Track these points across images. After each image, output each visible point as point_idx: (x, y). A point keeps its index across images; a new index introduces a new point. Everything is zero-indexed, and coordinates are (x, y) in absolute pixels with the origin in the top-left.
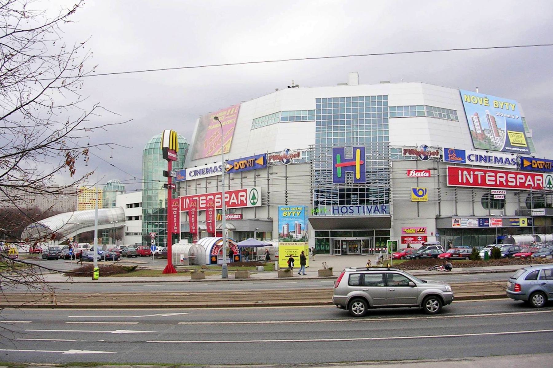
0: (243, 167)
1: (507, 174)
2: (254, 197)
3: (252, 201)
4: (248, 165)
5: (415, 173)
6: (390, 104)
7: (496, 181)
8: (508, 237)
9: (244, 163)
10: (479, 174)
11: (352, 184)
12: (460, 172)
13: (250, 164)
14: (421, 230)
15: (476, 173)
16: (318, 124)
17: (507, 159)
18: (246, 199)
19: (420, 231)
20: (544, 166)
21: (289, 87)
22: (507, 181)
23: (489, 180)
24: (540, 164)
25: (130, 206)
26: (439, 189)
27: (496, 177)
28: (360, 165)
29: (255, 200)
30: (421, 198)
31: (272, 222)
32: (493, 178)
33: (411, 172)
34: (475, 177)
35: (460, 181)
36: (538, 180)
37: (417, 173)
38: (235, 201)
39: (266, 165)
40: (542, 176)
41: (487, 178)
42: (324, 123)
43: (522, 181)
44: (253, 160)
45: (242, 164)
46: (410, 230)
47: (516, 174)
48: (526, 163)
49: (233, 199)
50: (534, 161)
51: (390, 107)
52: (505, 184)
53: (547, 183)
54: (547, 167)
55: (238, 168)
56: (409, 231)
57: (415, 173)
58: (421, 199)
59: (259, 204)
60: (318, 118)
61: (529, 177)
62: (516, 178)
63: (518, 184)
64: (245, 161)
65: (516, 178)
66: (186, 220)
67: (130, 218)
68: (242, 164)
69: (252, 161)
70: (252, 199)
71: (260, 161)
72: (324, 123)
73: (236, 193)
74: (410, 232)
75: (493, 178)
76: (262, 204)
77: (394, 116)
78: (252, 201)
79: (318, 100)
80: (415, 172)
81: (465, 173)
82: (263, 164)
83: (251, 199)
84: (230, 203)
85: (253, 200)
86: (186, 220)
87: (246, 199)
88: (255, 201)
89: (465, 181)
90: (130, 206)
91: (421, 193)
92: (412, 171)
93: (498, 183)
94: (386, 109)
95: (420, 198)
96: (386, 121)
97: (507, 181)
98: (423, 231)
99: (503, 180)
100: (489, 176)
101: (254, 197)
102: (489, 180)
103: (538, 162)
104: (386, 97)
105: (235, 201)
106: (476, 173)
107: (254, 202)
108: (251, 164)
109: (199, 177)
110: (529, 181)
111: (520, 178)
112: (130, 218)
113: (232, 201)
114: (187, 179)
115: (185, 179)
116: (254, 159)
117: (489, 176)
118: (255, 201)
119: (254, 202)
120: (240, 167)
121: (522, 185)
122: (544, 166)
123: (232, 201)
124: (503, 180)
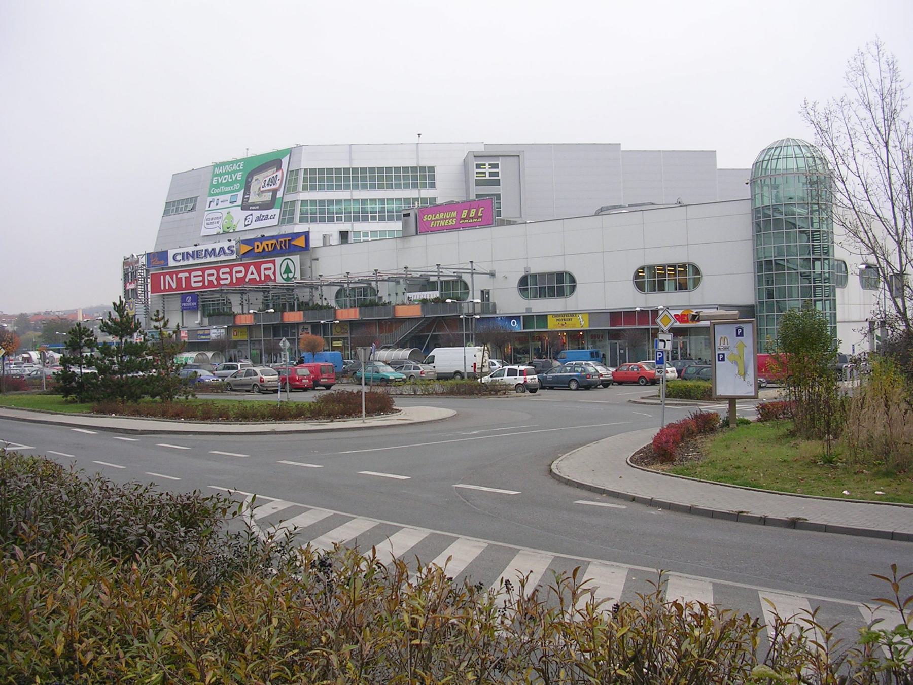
0: (270, 250)
3: (285, 276)
9: (272, 244)
18: (274, 273)
29: (289, 274)
38: (256, 276)
44: (287, 239)
45: (267, 245)
49: (252, 273)
64: (274, 241)
68: (267, 245)
69: (285, 241)
78: (285, 276)
83: (282, 273)
84: (247, 280)
85: (286, 275)
87: (274, 273)
88: (291, 275)
105: (256, 276)
107: (288, 276)
113: (249, 276)
116: (290, 238)
118: (291, 275)
119: (288, 276)
123: (249, 276)
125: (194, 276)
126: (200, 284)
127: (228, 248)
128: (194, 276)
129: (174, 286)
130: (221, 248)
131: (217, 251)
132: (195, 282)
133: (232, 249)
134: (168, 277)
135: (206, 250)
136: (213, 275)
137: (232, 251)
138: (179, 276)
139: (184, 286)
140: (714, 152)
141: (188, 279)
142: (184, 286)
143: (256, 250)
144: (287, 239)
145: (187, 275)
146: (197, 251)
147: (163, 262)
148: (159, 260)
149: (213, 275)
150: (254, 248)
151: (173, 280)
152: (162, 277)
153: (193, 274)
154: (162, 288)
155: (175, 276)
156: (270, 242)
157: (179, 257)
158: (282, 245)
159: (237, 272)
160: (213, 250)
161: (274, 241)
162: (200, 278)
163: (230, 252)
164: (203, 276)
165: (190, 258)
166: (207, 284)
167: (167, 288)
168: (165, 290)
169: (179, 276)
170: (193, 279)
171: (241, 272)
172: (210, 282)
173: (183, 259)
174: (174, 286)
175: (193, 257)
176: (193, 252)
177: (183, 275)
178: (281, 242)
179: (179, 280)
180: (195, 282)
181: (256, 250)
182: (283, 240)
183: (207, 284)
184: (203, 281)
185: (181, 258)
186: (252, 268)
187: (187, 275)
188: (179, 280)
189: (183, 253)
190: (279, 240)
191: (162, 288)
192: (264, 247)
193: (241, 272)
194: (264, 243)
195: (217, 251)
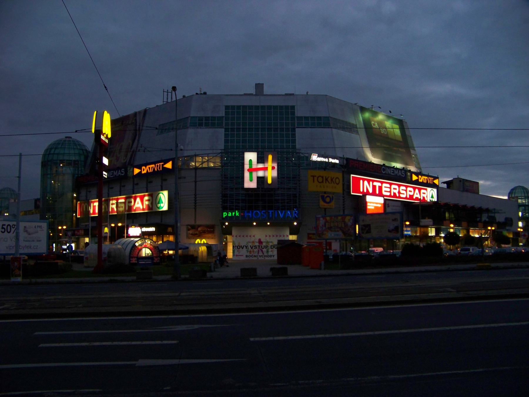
0: (151, 171)
7: (390, 192)
9: (152, 167)
12: (361, 181)
15: (375, 183)
16: (226, 130)
22: (399, 193)
23: (385, 191)
24: (424, 179)
26: (343, 197)
27: (390, 188)
30: (329, 204)
32: (389, 190)
34: (374, 187)
35: (361, 190)
36: (424, 193)
40: (426, 189)
41: (384, 189)
42: (233, 130)
43: (412, 194)
51: (297, 117)
52: (397, 195)
53: (430, 197)
54: (430, 182)
60: (227, 124)
61: (417, 191)
62: (406, 191)
63: (408, 197)
65: (406, 191)
69: (160, 165)
72: (233, 130)
75: (389, 190)
77: (300, 126)
79: (227, 107)
81: (366, 182)
91: (328, 200)
93: (392, 194)
94: (293, 119)
95: (327, 205)
96: (294, 130)
97: (399, 193)
99: (396, 192)
100: (385, 187)
102: (385, 191)
104: (293, 107)
106: (375, 183)
110: (417, 194)
111: (410, 191)
117: (385, 187)
124: (396, 192)
144: (161, 164)
161: (153, 166)
182: (158, 164)
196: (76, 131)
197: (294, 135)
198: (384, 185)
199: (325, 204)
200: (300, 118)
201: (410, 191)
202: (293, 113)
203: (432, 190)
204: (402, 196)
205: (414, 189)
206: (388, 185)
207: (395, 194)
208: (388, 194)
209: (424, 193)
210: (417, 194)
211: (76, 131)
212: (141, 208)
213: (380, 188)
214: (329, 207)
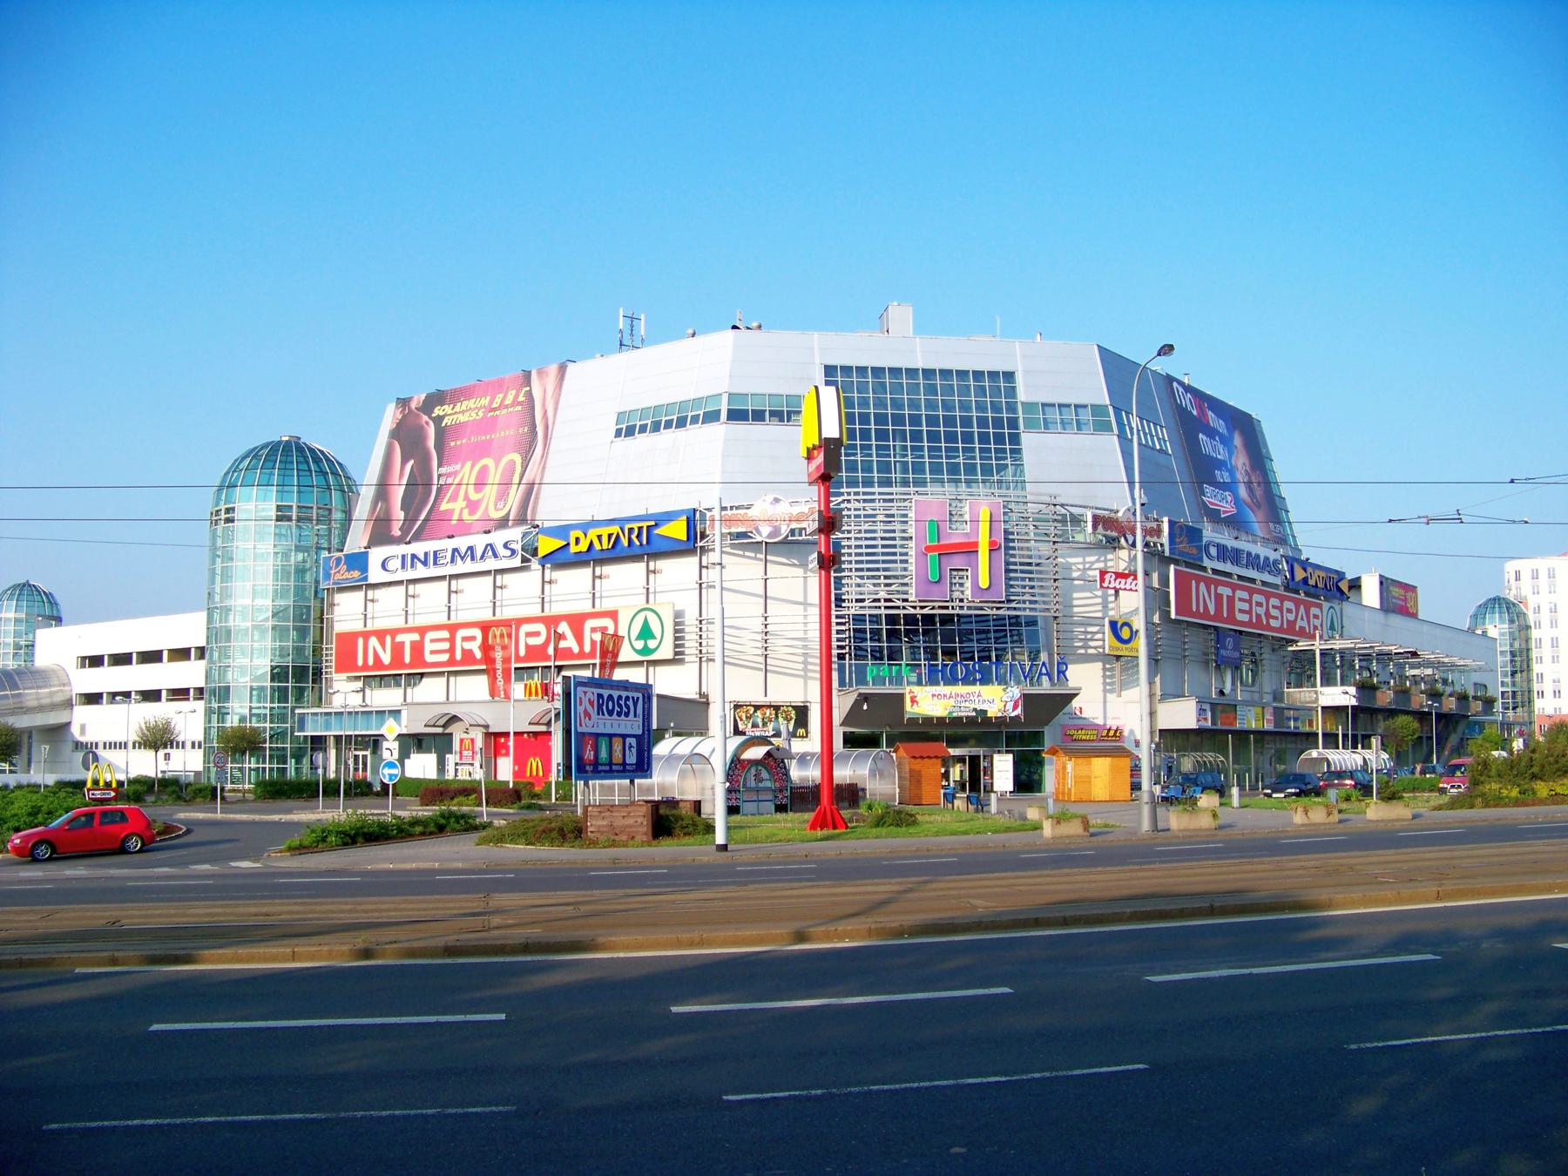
0: (605, 547)
1: (1268, 596)
2: (646, 632)
3: (639, 645)
4: (625, 542)
5: (1115, 580)
6: (1022, 396)
8: (1310, 754)
9: (610, 536)
10: (1225, 591)
11: (965, 600)
13: (634, 537)
14: (1112, 733)
17: (1267, 559)
19: (1107, 735)
20: (1326, 584)
21: (735, 327)
25: (96, 661)
27: (1249, 602)
28: (990, 550)
30: (1128, 646)
31: (708, 704)
32: (1246, 606)
33: (1107, 577)
36: (1316, 617)
37: (1118, 580)
39: (693, 542)
40: (1319, 606)
41: (1239, 605)
43: (1291, 617)
44: (644, 524)
45: (599, 537)
46: (1083, 732)
47: (1282, 599)
48: (1300, 574)
50: (1310, 570)
55: (583, 547)
56: (1081, 735)
57: (1115, 580)
58: (1126, 649)
59: (666, 652)
62: (1280, 609)
64: (615, 529)
66: (405, 700)
67: (93, 699)
68: (599, 537)
69: (640, 529)
70: (637, 639)
71: (677, 530)
73: (576, 622)
74: (1084, 737)
75: (1246, 606)
76: (676, 653)
77: (1031, 425)
78: (639, 645)
80: (1114, 576)
81: (1202, 586)
82: (684, 538)
83: (633, 638)
86: (405, 700)
88: (652, 644)
89: (1202, 611)
90: (96, 661)
91: (1125, 634)
92: (1110, 574)
94: (1012, 408)
95: (1124, 646)
96: (1015, 439)
97: (1267, 614)
98: (1115, 735)
99: (1261, 611)
101: (646, 632)
103: (1318, 572)
104: (1009, 376)
108: (638, 536)
109: (421, 571)
110: (1302, 619)
111: (1289, 611)
112: (93, 699)
114: (371, 580)
115: (366, 579)
116: (653, 523)
118: (652, 644)
120: (591, 543)
121: (1292, 624)
122: (1326, 584)
124: (1261, 611)
125: (433, 641)
126: (445, 657)
127: (506, 546)
128: (433, 641)
129: (386, 658)
130: (487, 545)
131: (479, 553)
132: (433, 652)
133: (512, 546)
134: (373, 641)
135: (455, 550)
136: (473, 638)
137: (513, 552)
138: (399, 638)
139: (407, 660)
140: (1416, 587)
141: (418, 648)
142: (407, 660)
143: (573, 549)
144: (644, 524)
145: (415, 637)
146: (435, 553)
147: (356, 574)
148: (348, 570)
149: (473, 638)
150: (568, 544)
151: (384, 649)
152: (360, 641)
153: (430, 635)
154: (360, 663)
155: (388, 639)
156: (605, 531)
157: (394, 564)
158: (634, 537)
159: (529, 634)
160: (471, 548)
162: (446, 645)
163: (509, 553)
164: (452, 640)
165: (419, 565)
166: (458, 656)
167: (371, 662)
168: (365, 667)
169: (399, 638)
170: (428, 647)
171: (537, 634)
172: (468, 655)
173: (403, 567)
174: (386, 658)
175: (425, 563)
176: (426, 554)
177: (407, 639)
178: (631, 530)
179: (398, 649)
180: (433, 652)
181: (573, 549)
182: (635, 526)
183: (458, 656)
184: (452, 650)
185: (399, 566)
186: (563, 627)
187: (415, 637)
188: (398, 649)
189: (404, 557)
190: (627, 527)
191: (360, 663)
192: (591, 542)
193: (537, 634)
194: (593, 534)
195: (479, 553)
196: (1512, 481)
197: (1017, 452)
198: (1240, 594)
199: (1120, 645)
200: (1029, 407)
201: (1289, 611)
202: (1012, 392)
203: (1331, 607)
204: (1273, 623)
205: (1297, 603)
206: (1245, 595)
207: (1258, 616)
208: (1245, 618)
209: (1316, 617)
210: (1302, 619)
211: (1512, 481)
212: (576, 649)
213: (1231, 600)
214: (1127, 653)
